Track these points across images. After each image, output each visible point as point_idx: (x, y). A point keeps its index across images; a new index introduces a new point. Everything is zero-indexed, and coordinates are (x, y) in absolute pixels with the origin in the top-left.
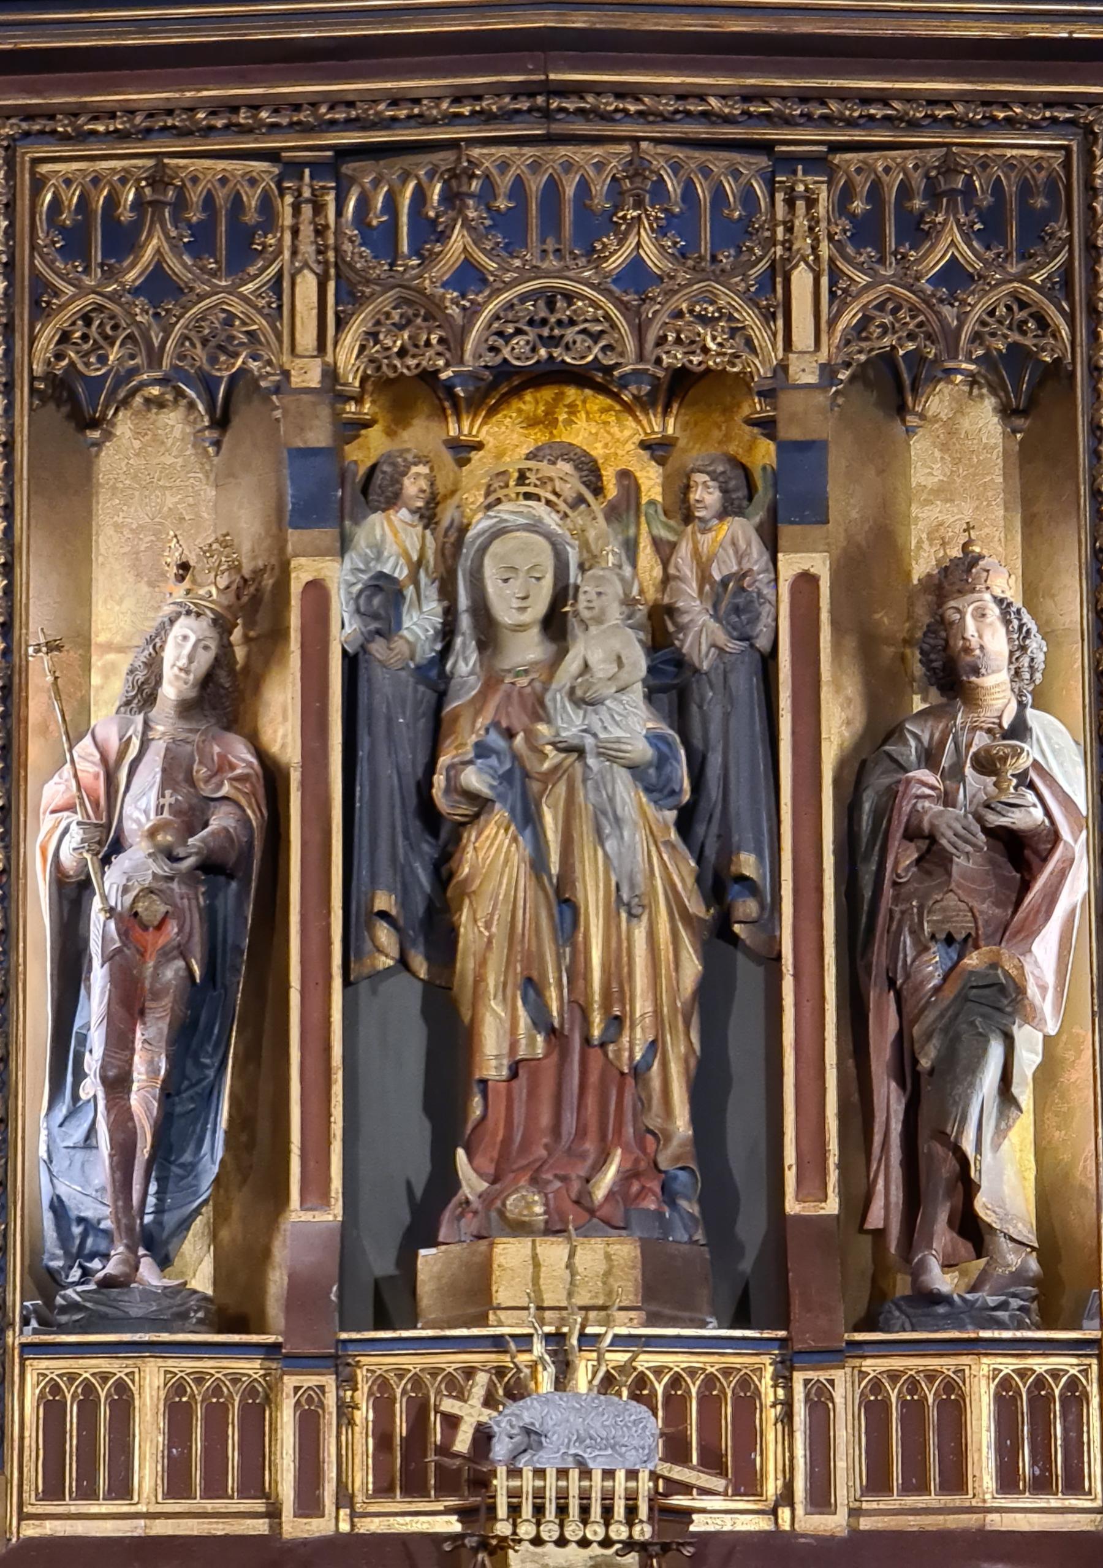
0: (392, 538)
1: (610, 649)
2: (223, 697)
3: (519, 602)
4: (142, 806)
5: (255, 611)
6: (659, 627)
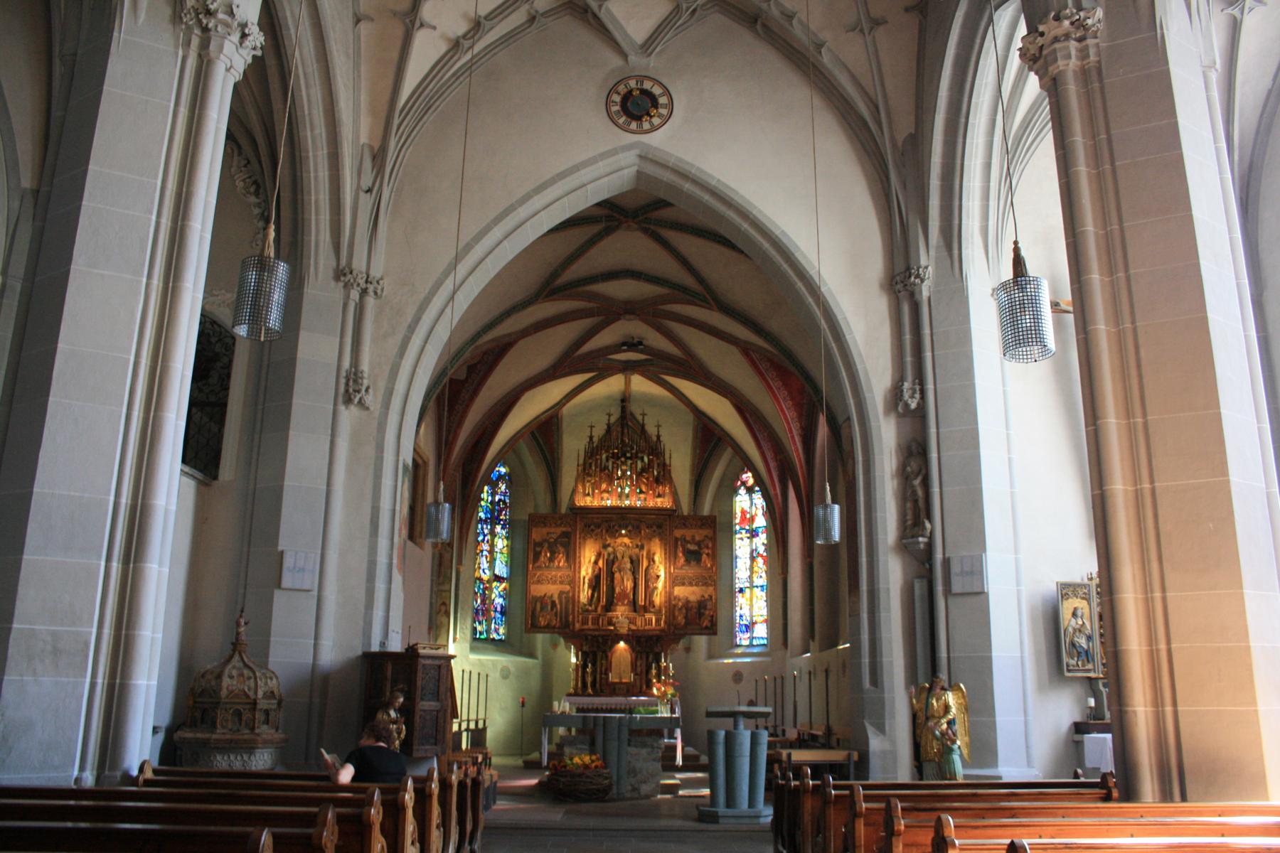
0: (610, 549)
1: (627, 560)
2: (596, 563)
3: (619, 556)
4: (590, 571)
5: (599, 555)
6: (631, 558)
